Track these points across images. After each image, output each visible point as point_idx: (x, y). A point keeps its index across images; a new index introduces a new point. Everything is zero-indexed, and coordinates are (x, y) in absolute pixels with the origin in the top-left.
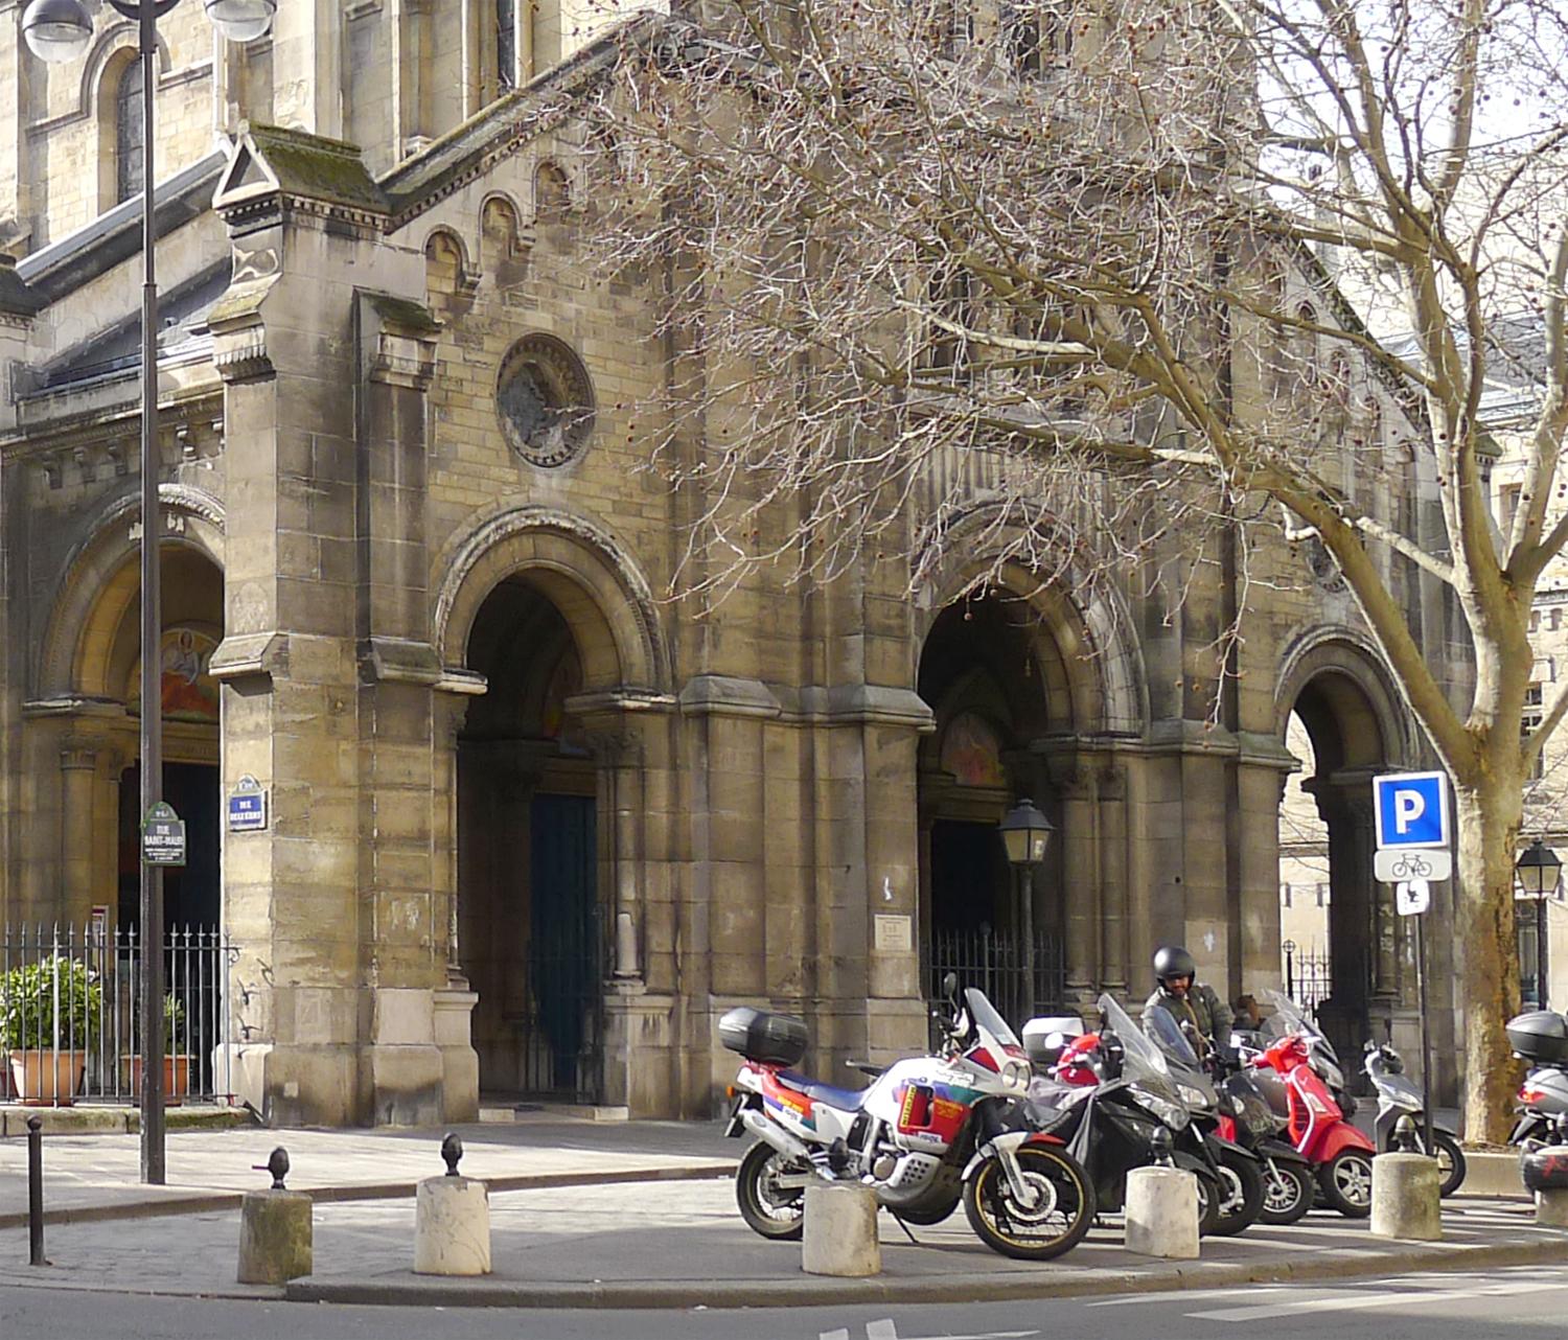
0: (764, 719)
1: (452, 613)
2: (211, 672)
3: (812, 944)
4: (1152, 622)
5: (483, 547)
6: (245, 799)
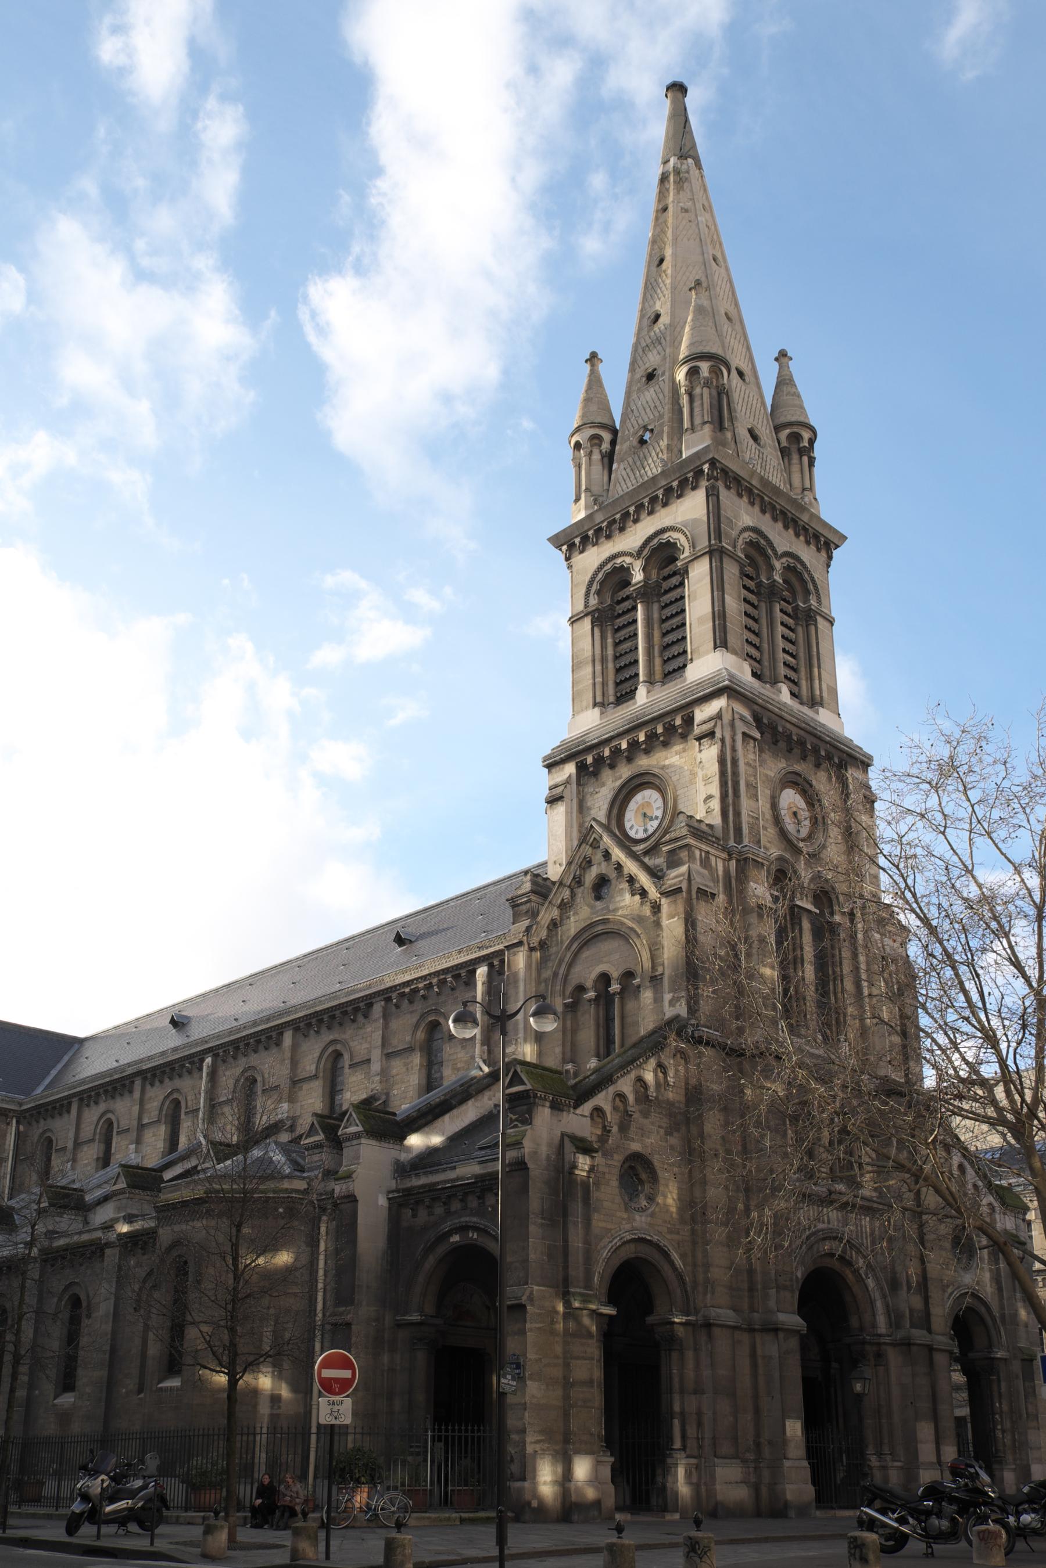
0: (735, 1328)
1: (602, 1278)
3: (758, 1435)
4: (894, 1285)
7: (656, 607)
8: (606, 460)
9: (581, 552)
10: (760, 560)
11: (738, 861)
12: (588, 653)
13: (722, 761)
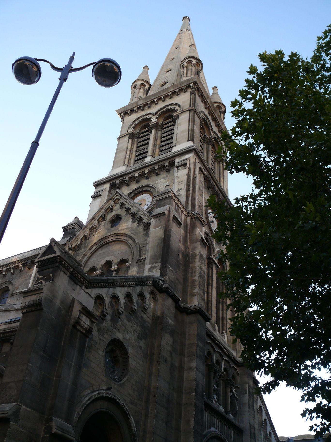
5: (93, 398)
7: (160, 132)
8: (146, 92)
9: (129, 116)
10: (206, 130)
11: (192, 218)
12: (125, 147)
13: (188, 176)
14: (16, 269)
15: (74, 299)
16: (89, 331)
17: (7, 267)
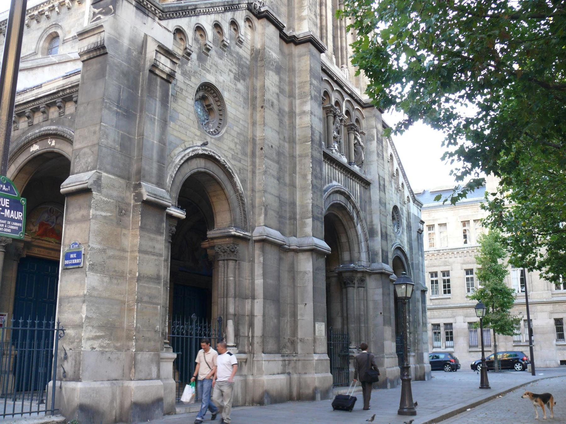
2: (62, 190)
5: (187, 157)
6: (73, 253)
14: (62, 6)
15: (146, 36)
16: (171, 76)
17: (49, 4)
